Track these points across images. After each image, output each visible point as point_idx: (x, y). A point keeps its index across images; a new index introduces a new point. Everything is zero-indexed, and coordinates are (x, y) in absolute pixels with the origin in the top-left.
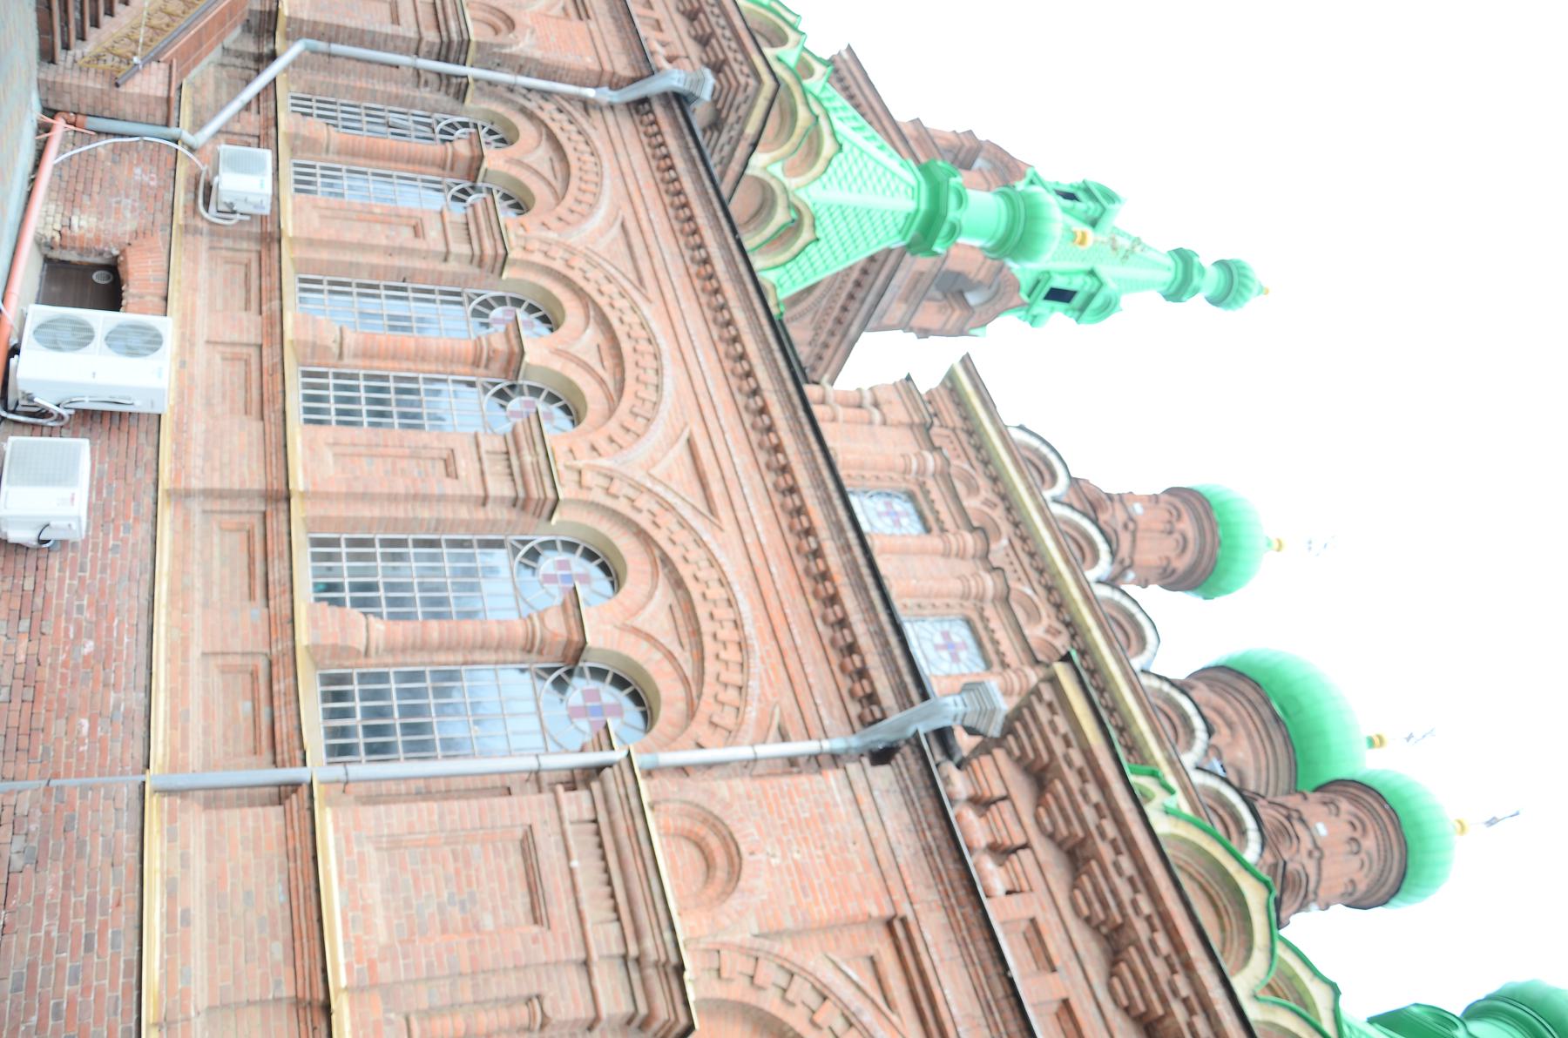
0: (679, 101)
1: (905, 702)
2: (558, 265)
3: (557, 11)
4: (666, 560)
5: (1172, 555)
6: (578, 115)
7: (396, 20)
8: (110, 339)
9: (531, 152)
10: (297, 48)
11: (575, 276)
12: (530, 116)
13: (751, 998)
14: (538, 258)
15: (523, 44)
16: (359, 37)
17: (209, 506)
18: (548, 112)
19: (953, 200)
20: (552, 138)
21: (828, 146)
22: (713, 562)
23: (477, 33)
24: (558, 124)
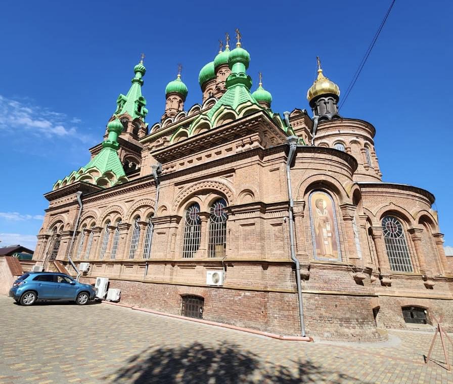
0: (82, 197)
1: (153, 178)
2: (102, 219)
3: (68, 215)
4: (138, 208)
5: (176, 101)
6: (83, 213)
7: (66, 242)
8: (98, 285)
9: (88, 222)
10: (69, 257)
11: (104, 217)
12: (83, 221)
13: (178, 206)
14: (101, 222)
15: (72, 222)
16: (68, 248)
17: (122, 272)
18: (82, 218)
19: (109, 143)
20: (86, 218)
21: (95, 168)
22: (138, 202)
23: (69, 229)
24: (84, 216)
